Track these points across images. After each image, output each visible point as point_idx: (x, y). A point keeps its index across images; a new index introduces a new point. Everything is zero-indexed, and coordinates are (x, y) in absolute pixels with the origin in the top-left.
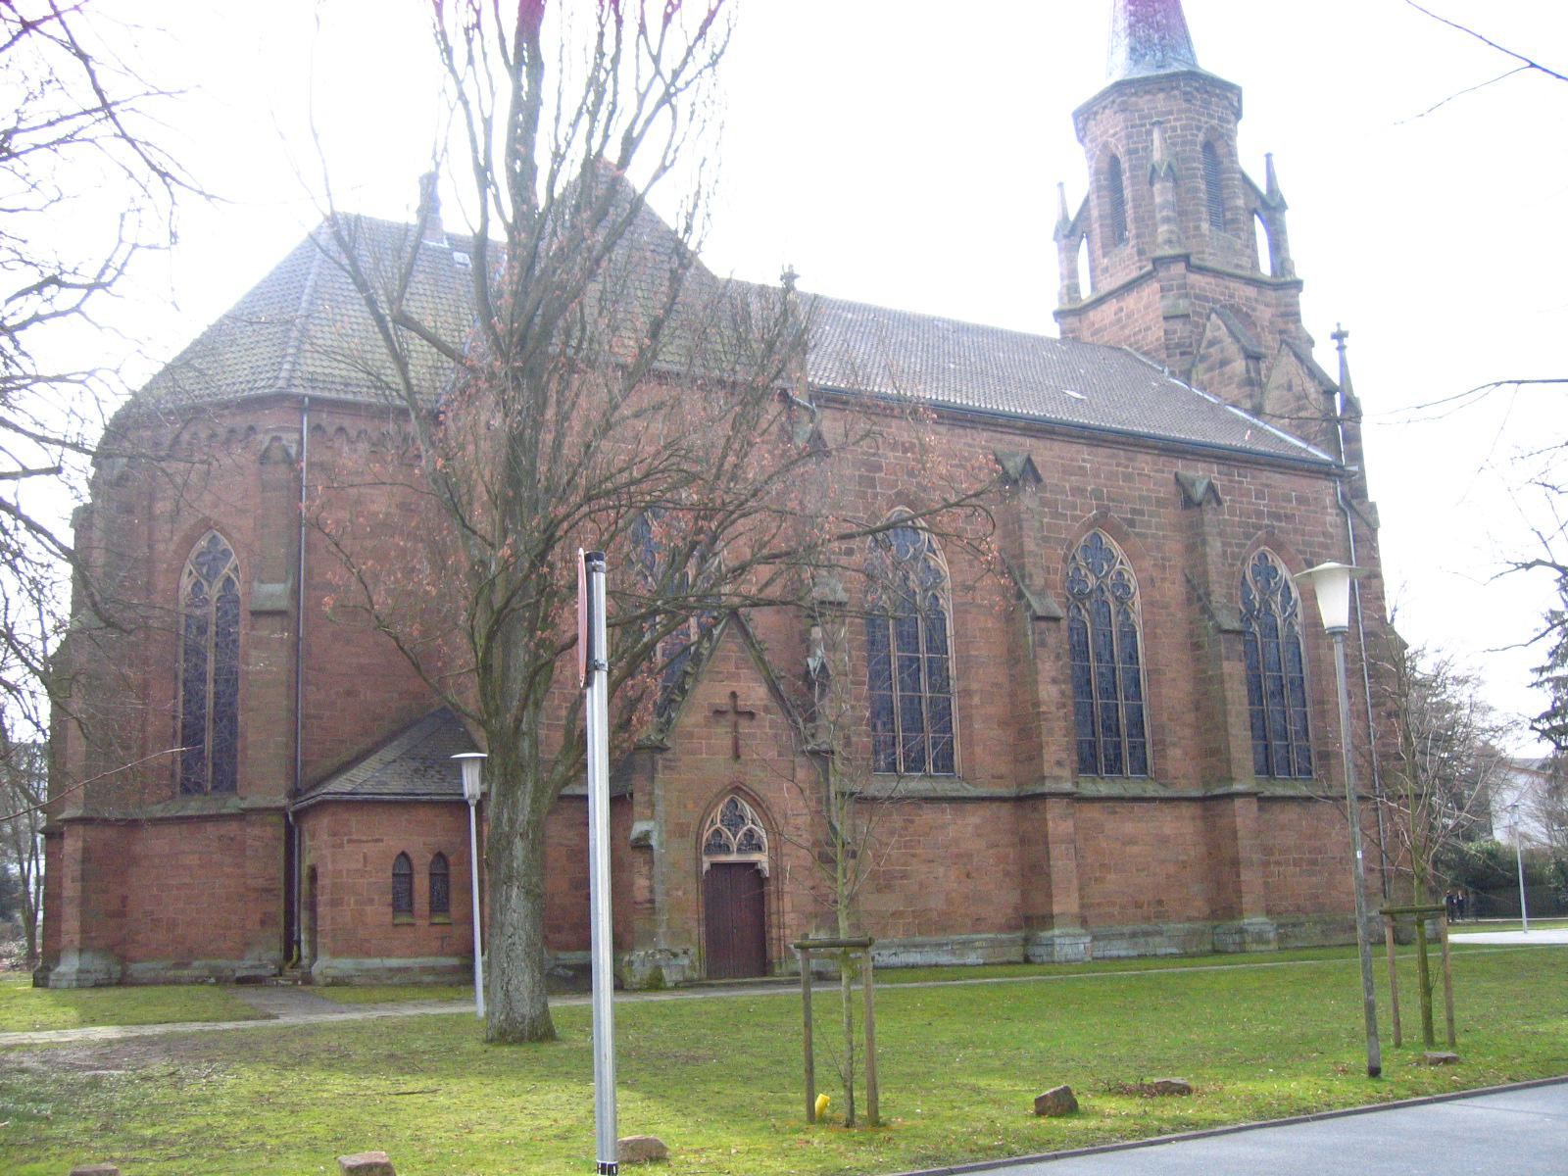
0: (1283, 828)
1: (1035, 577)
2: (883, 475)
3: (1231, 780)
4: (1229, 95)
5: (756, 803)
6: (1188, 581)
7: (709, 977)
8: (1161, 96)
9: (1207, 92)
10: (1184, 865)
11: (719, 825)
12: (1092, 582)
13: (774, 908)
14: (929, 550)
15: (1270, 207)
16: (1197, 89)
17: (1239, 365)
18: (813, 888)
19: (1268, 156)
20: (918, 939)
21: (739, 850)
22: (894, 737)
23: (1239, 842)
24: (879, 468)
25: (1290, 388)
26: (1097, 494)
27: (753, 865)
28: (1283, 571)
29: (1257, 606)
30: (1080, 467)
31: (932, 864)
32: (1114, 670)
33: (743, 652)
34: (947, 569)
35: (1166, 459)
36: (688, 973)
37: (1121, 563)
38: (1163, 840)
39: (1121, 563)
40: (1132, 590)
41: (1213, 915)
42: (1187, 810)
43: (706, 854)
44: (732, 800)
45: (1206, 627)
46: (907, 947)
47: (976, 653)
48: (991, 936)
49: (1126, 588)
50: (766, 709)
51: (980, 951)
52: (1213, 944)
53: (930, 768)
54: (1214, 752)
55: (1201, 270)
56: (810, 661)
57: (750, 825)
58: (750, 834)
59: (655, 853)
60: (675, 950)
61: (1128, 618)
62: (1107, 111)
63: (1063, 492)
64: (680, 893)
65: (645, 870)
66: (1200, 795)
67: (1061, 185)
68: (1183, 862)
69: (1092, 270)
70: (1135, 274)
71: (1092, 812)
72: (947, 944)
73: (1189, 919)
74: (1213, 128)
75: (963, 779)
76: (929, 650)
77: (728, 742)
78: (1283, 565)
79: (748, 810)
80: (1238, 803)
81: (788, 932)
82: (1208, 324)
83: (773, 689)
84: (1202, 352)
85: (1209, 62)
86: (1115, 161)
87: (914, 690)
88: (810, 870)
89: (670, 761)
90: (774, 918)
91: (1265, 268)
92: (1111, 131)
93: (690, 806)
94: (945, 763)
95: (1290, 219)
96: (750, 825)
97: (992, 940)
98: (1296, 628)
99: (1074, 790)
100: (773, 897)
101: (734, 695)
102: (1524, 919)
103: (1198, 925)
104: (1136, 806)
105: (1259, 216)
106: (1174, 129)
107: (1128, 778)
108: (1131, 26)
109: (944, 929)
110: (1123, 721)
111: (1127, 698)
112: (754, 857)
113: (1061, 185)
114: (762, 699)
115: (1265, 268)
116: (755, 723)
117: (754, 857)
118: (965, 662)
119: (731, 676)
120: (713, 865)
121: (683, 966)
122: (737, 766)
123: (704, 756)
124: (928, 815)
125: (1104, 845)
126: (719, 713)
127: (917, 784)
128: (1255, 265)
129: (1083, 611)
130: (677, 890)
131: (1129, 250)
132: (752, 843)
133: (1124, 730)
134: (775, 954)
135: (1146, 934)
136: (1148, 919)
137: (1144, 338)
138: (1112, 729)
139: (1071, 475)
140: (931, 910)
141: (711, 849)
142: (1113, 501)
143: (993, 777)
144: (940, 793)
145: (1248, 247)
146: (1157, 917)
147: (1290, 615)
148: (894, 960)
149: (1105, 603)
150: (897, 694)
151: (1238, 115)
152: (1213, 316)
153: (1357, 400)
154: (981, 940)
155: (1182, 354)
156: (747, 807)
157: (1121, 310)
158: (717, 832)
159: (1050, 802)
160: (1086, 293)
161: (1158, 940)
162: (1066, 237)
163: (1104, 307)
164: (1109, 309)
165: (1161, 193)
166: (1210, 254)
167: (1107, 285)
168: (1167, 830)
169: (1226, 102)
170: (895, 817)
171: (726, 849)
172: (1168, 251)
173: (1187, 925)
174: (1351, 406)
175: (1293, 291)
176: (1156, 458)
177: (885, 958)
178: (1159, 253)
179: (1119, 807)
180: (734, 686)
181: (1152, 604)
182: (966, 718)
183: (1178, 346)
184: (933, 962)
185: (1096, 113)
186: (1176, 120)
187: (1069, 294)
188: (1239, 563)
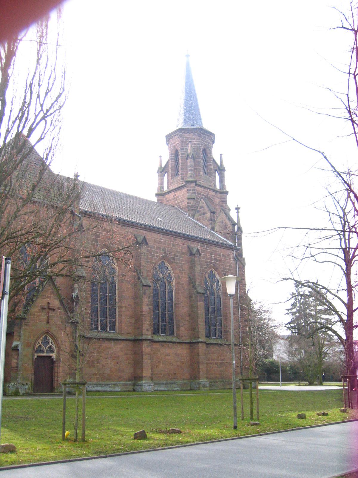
0: (213, 353)
1: (144, 273)
3: (198, 338)
4: (211, 136)
5: (53, 337)
6: (189, 277)
7: (34, 392)
8: (192, 134)
9: (205, 134)
10: (183, 363)
11: (41, 344)
12: (161, 276)
13: (56, 371)
15: (221, 170)
16: (202, 133)
17: (208, 215)
18: (69, 365)
19: (221, 155)
20: (101, 382)
21: (46, 352)
22: (97, 319)
23: (200, 357)
24: (99, 237)
25: (223, 223)
26: (164, 249)
27: (50, 357)
28: (217, 276)
29: (209, 286)
30: (160, 241)
31: (106, 359)
32: (166, 302)
33: (53, 290)
34: (117, 269)
35: (185, 240)
36: (27, 391)
37: (170, 271)
38: (177, 355)
40: (173, 279)
41: (191, 378)
42: (185, 346)
43: (36, 353)
44: (45, 336)
45: (194, 291)
46: (97, 385)
49: (171, 278)
50: (59, 308)
52: (190, 387)
53: (108, 329)
54: (194, 329)
55: (200, 186)
56: (73, 294)
57: (51, 344)
58: (50, 347)
59: (20, 352)
60: (24, 383)
61: (171, 287)
62: (176, 137)
63: (155, 248)
64: (27, 365)
65: (16, 357)
66: (189, 342)
67: (161, 157)
68: (183, 362)
69: (168, 183)
70: (180, 185)
71: (157, 346)
72: (110, 384)
73: (184, 379)
74: (206, 145)
75: (118, 333)
76: (110, 293)
77: (46, 318)
78: (217, 275)
79: (50, 340)
80: (200, 345)
81: (60, 379)
82: (200, 202)
83: (61, 302)
84: (198, 210)
85: (207, 125)
86: (177, 152)
87: (105, 305)
88: (68, 359)
89: (26, 322)
90: (56, 374)
91: (218, 187)
92: (177, 143)
93: (32, 337)
94: (113, 329)
95: (227, 174)
96: (51, 344)
98: (220, 293)
99: (151, 338)
100: (56, 367)
101: (48, 303)
102: (281, 382)
103: (186, 381)
104: (170, 345)
105: (217, 172)
106: (195, 144)
107: (168, 336)
108: (185, 113)
110: (167, 318)
111: (169, 311)
112: (51, 355)
113: (161, 157)
114: (58, 305)
115: (218, 187)
116: (54, 312)
117: (51, 355)
118: (121, 297)
119: (48, 297)
120: (38, 356)
121: (26, 388)
122: (48, 326)
123: (38, 322)
124: (107, 344)
125: (159, 356)
126: (43, 308)
127: (104, 334)
128: (215, 186)
129: (158, 284)
130: (26, 364)
131: (179, 178)
132: (51, 350)
133: (167, 321)
134: (55, 386)
135: (171, 383)
136: (171, 379)
137: (181, 204)
138: (164, 320)
140: (105, 373)
141: (37, 351)
142: (169, 252)
143: (127, 333)
144: (111, 337)
145: (213, 180)
146: (174, 378)
147: (218, 289)
148: (93, 389)
149: (165, 282)
150: (99, 306)
151: (213, 142)
152: (202, 200)
153: (241, 227)
155: (192, 210)
156: (50, 339)
157: (175, 195)
158: (40, 346)
159: (144, 342)
160: (165, 189)
161: (174, 385)
162: (161, 172)
163: (170, 194)
164: (172, 195)
165: (190, 162)
166: (203, 181)
167: (172, 188)
168: (178, 352)
169: (210, 138)
171: (42, 351)
172: (190, 179)
173: (183, 381)
174: (240, 229)
175: (225, 195)
176: (182, 240)
177: (90, 388)
178: (188, 180)
179: (164, 344)
180: (49, 300)
181: (178, 283)
182: (120, 315)
183: (191, 207)
184: (105, 390)
185: (173, 137)
186: (196, 141)
187: (160, 189)
188: (205, 273)
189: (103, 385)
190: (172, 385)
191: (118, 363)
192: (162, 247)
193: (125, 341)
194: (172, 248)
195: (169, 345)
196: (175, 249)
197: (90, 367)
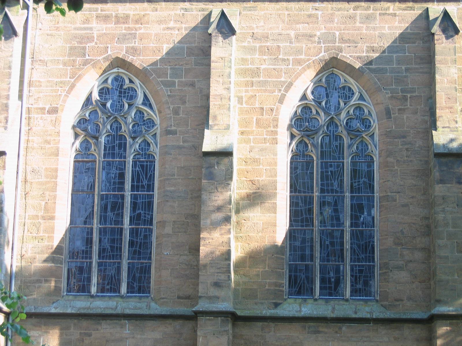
1: (219, 117)
2: (93, 44)
14: (144, 104)
24: (90, 39)
30: (310, 16)
39: (361, 98)
47: (173, 188)
53: (124, 289)
87: (117, 222)
139: (298, 23)
143: (179, 297)
144: (119, 311)
159: (202, 320)
170: (72, 330)
179: (323, 327)
192: (318, 33)
194: (359, 29)
195: (340, 328)
196: (374, 29)
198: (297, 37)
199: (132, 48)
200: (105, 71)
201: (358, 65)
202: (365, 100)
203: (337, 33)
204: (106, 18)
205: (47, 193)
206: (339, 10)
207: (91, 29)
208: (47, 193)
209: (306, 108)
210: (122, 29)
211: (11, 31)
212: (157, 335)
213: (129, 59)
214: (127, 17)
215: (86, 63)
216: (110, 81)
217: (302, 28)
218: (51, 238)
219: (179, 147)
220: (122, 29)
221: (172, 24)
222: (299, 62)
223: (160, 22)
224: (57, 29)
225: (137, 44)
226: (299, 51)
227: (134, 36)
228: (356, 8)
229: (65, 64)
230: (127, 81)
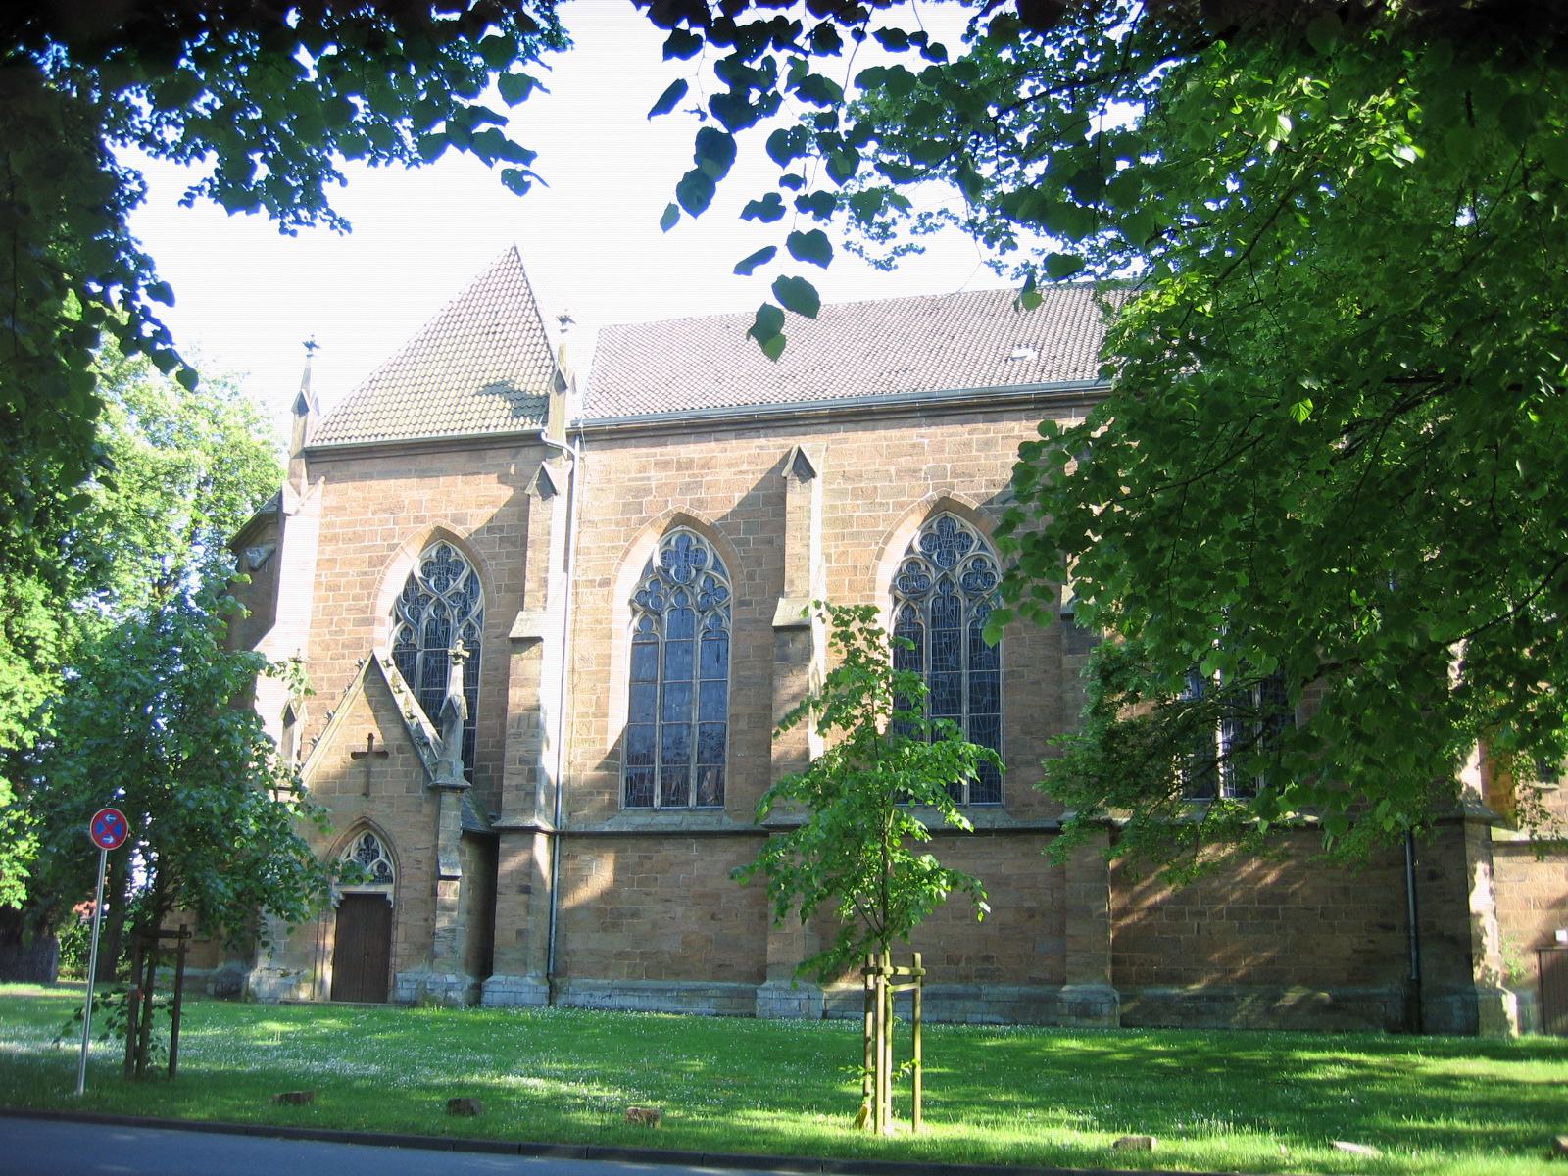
1: (796, 582)
10: (1031, 914)
14: (715, 569)
20: (643, 982)
24: (647, 491)
27: (384, 895)
30: (914, 446)
39: (982, 547)
46: (624, 990)
48: (733, 985)
50: (400, 749)
51: (713, 1000)
72: (672, 990)
73: (1033, 981)
81: (398, 961)
97: (731, 989)
109: (677, 975)
116: (387, 762)
124: (669, 851)
132: (383, 876)
135: (953, 996)
136: (966, 978)
140: (662, 952)
142: (958, 476)
144: (684, 828)
146: (982, 977)
148: (608, 1002)
154: (718, 988)
161: (969, 1004)
168: (1006, 869)
173: (1025, 989)
189: (644, 990)
190: (959, 1004)
191: (713, 917)
192: (924, 467)
193: (744, 839)
194: (977, 458)
195: (954, 843)
197: (605, 930)
198: (898, 472)
199: (698, 500)
200: (666, 531)
201: (974, 505)
202: (986, 549)
203: (949, 466)
204: (665, 465)
205: (599, 685)
206: (950, 436)
207: (649, 479)
208: (599, 685)
209: (912, 564)
210: (685, 477)
211: (549, 490)
212: (730, 856)
213: (694, 513)
214: (692, 460)
215: (642, 522)
216: (673, 542)
217: (904, 462)
218: (603, 740)
219: (756, 621)
220: (685, 477)
221: (744, 467)
222: (900, 506)
223: (730, 465)
224: (609, 481)
225: (702, 494)
226: (901, 492)
227: (699, 485)
228: (971, 433)
229: (618, 524)
230: (694, 541)
